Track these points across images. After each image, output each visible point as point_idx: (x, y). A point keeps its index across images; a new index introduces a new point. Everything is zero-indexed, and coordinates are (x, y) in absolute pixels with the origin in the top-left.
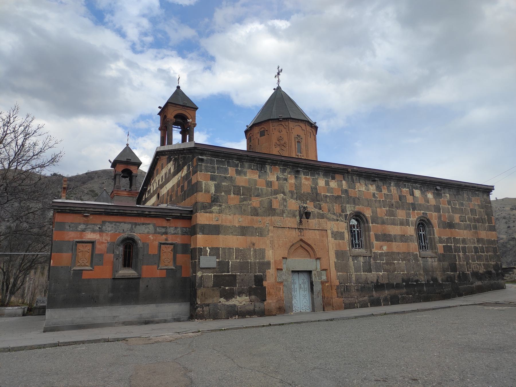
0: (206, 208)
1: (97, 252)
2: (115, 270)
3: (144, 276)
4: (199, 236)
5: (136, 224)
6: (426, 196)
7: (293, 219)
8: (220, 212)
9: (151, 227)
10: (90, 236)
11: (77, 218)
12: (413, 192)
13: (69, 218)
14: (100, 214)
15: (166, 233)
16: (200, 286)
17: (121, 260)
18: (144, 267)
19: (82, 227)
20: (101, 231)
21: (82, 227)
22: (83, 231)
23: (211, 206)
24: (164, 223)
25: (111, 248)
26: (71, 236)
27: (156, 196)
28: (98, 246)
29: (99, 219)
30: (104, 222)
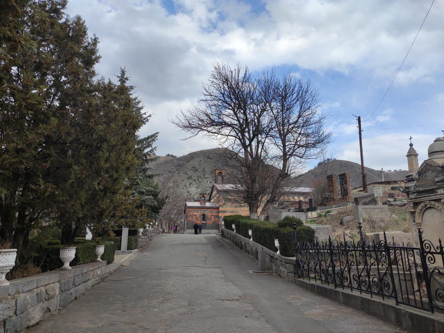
0: (222, 206)
1: (197, 217)
2: (201, 222)
3: (207, 223)
4: (220, 213)
5: (205, 211)
6: (300, 198)
7: (247, 208)
8: (226, 207)
9: (209, 211)
10: (195, 214)
11: (192, 209)
12: (294, 197)
13: (191, 210)
14: (197, 208)
15: (212, 213)
16: (220, 226)
17: (202, 219)
18: (207, 221)
19: (194, 211)
20: (198, 212)
21: (194, 211)
22: (194, 212)
23: (223, 206)
24: (212, 210)
25: (200, 216)
26: (191, 214)
27: (213, 199)
28: (197, 216)
29: (197, 210)
30: (198, 210)
